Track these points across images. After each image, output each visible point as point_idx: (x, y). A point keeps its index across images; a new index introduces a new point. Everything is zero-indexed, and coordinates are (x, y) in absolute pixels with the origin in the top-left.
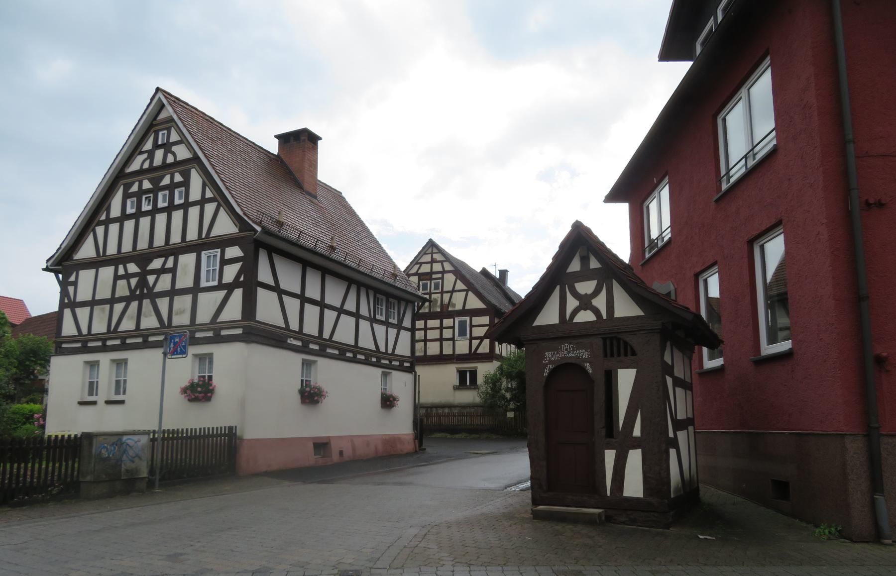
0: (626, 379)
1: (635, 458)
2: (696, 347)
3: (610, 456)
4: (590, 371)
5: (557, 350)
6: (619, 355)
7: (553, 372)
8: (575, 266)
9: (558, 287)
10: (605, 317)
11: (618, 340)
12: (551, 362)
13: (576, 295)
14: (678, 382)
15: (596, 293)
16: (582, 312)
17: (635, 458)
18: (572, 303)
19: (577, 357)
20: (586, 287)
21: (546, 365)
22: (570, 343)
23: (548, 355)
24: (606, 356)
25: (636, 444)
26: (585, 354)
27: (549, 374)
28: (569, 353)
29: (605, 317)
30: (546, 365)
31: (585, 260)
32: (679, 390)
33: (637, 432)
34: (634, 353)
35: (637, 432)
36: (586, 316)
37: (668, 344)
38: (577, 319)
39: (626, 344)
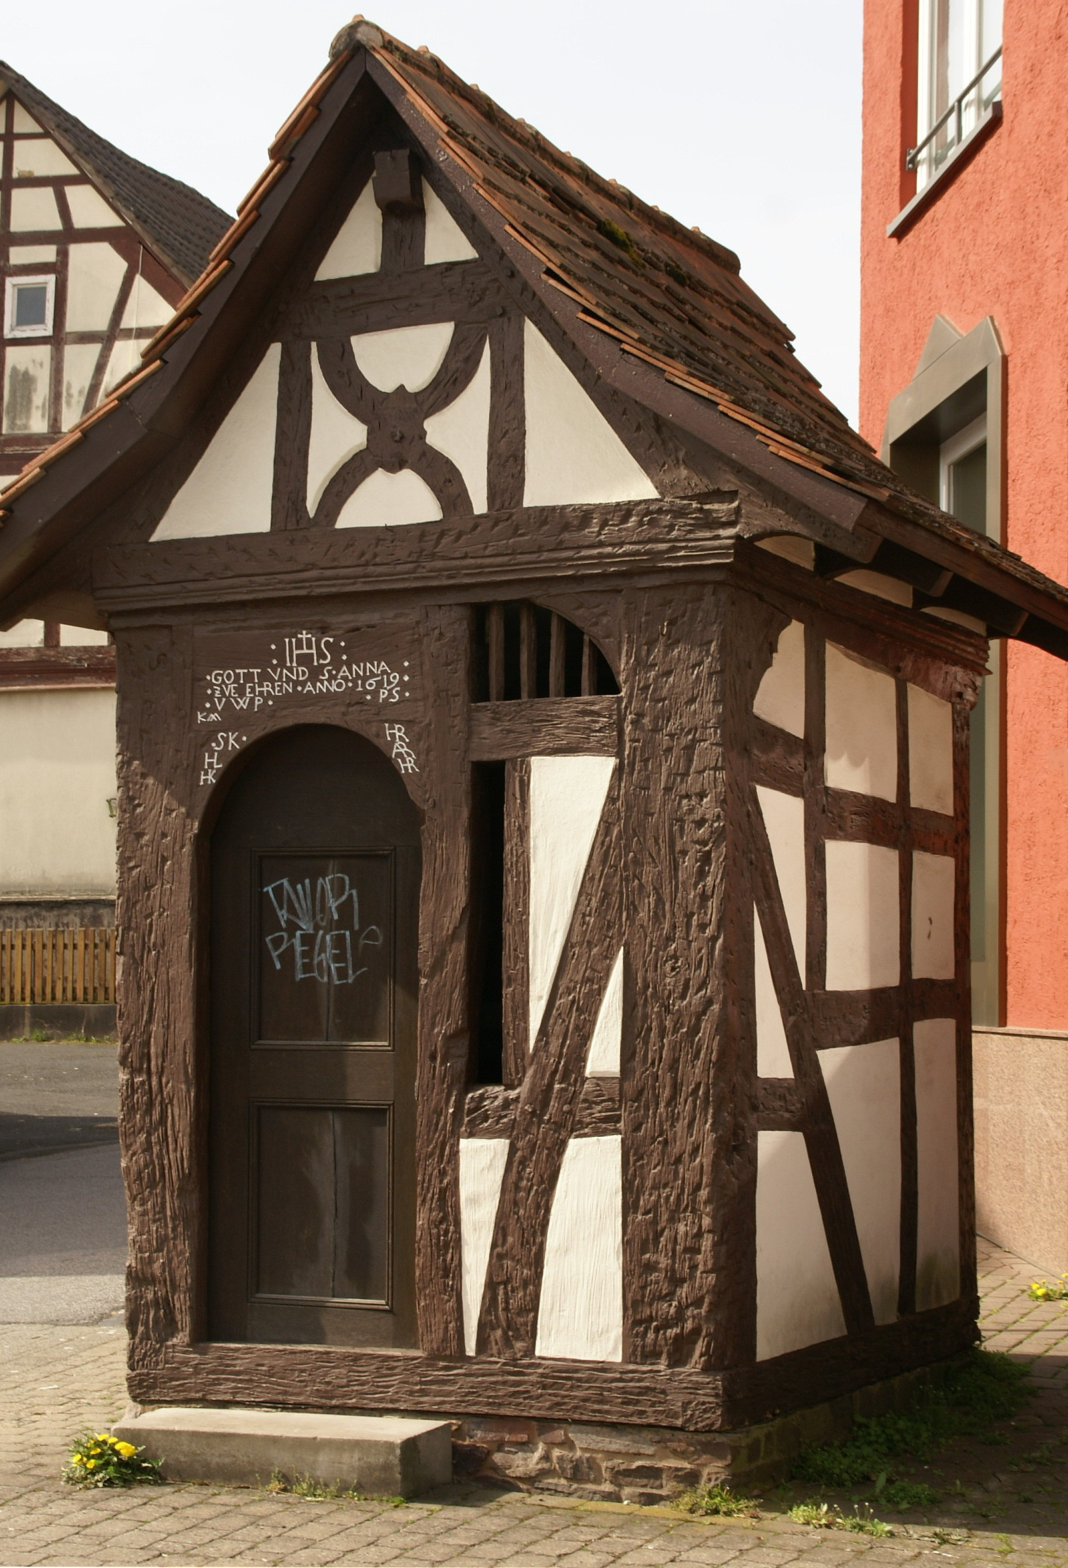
0: (566, 801)
1: (591, 1172)
2: (994, 644)
4: (408, 765)
5: (262, 658)
6: (541, 690)
7: (240, 769)
8: (356, 249)
9: (275, 351)
10: (480, 505)
11: (542, 617)
12: (233, 719)
13: (354, 393)
14: (829, 816)
15: (448, 384)
16: (379, 477)
17: (591, 1172)
20: (400, 357)
21: (211, 732)
22: (324, 630)
23: (222, 683)
24: (480, 692)
27: (224, 778)
28: (315, 674)
29: (480, 505)
30: (211, 732)
31: (403, 219)
32: (849, 860)
33: (604, 1055)
34: (606, 683)
35: (604, 1055)
36: (394, 501)
37: (792, 637)
38: (351, 516)
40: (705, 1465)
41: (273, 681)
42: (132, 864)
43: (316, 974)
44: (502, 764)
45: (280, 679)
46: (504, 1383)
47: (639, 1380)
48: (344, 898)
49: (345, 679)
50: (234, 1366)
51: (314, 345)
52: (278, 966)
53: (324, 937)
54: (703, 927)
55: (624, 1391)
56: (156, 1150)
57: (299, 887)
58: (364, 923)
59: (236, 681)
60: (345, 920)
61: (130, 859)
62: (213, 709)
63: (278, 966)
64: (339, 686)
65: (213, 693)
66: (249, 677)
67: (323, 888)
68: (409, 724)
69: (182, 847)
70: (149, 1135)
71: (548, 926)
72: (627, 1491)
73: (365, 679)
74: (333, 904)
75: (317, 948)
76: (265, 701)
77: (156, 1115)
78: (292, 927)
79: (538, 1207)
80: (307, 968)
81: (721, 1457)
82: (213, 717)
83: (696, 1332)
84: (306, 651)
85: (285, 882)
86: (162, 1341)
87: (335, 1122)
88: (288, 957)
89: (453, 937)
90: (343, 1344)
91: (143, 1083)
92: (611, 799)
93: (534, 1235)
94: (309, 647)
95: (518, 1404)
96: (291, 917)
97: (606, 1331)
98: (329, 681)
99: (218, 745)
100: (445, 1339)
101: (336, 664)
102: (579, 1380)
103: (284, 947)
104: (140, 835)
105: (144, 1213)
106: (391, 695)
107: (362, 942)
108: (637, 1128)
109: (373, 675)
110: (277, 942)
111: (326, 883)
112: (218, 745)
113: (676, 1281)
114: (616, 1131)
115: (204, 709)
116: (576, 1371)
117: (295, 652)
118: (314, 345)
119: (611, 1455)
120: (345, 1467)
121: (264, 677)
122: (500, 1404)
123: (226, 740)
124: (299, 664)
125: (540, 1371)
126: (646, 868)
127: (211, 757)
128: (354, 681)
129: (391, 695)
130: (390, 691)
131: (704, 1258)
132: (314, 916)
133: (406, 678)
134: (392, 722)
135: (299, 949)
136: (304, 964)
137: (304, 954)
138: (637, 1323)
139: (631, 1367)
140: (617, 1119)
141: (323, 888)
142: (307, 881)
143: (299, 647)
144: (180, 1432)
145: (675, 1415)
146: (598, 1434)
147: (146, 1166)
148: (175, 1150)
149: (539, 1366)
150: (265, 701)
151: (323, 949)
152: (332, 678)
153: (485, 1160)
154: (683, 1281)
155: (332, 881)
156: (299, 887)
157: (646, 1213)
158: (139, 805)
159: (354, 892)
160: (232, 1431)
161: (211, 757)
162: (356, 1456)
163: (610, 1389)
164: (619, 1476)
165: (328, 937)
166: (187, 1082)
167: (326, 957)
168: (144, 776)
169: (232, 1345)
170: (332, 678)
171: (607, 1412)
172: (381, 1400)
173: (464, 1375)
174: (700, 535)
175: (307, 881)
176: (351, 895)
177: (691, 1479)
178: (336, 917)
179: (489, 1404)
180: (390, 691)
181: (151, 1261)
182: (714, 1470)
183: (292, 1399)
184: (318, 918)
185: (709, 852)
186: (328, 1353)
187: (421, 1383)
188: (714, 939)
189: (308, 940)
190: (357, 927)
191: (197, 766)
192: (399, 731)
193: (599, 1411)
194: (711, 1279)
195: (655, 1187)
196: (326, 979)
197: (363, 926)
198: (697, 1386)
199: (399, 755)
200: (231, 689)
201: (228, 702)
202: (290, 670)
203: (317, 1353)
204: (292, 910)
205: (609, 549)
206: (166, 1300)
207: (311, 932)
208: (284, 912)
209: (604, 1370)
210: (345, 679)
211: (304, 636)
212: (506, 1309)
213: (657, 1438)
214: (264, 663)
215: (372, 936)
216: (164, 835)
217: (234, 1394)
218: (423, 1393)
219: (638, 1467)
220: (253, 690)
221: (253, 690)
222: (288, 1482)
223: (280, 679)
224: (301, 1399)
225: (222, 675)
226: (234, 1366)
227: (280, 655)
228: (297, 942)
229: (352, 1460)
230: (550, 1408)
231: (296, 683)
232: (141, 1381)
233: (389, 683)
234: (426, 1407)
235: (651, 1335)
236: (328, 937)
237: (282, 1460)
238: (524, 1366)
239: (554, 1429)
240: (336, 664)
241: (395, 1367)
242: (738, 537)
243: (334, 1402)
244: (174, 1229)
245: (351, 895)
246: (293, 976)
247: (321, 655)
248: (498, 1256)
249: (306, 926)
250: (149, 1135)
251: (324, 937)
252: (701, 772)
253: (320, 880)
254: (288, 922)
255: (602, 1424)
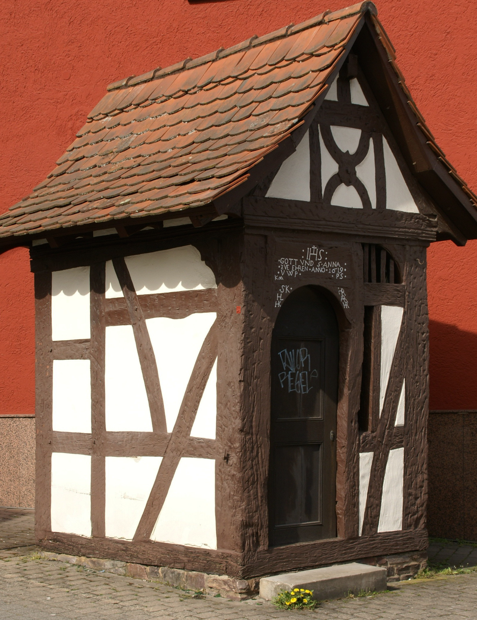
3: (366, 460)
4: (346, 305)
5: (298, 255)
10: (374, 206)
12: (288, 280)
18: (329, 167)
19: (327, 276)
23: (284, 263)
25: (397, 438)
26: (338, 270)
27: (284, 304)
29: (374, 206)
33: (400, 420)
35: (400, 420)
36: (346, 198)
39: (389, 257)
40: (421, 562)
41: (301, 265)
42: (248, 341)
43: (296, 390)
44: (373, 307)
45: (304, 265)
46: (369, 545)
47: (407, 536)
48: (306, 358)
49: (325, 267)
50: (282, 556)
51: (319, 125)
52: (282, 387)
53: (299, 374)
54: (424, 371)
55: (403, 540)
56: (255, 468)
57: (290, 353)
58: (312, 369)
59: (289, 264)
60: (306, 368)
61: (248, 338)
62: (280, 275)
63: (282, 387)
64: (323, 270)
65: (281, 268)
66: (293, 262)
67: (299, 354)
68: (346, 289)
69: (268, 334)
70: (252, 461)
71: (385, 370)
72: (402, 576)
73: (332, 268)
74: (302, 360)
75: (296, 379)
76: (299, 274)
77: (255, 453)
78: (288, 370)
79: (381, 476)
80: (293, 387)
81: (425, 558)
82: (281, 278)
83: (422, 516)
84: (314, 254)
85: (286, 350)
86: (255, 551)
87: (302, 450)
88: (286, 382)
89: (358, 375)
90: (306, 541)
91: (250, 439)
92: (403, 323)
93: (379, 487)
94: (315, 253)
95: (373, 552)
96: (288, 366)
97: (398, 520)
98: (320, 267)
99: (282, 291)
100: (354, 532)
101: (323, 261)
102: (391, 539)
103: (285, 378)
104: (252, 328)
105: (249, 496)
106: (340, 276)
107: (311, 376)
108: (407, 445)
109: (335, 267)
110: (282, 376)
111: (300, 351)
112: (282, 291)
113: (416, 498)
114: (402, 446)
115: (277, 274)
116: (390, 536)
117: (310, 254)
118: (319, 125)
119: (397, 564)
120: (370, 583)
121: (299, 263)
122: (368, 553)
123: (285, 288)
124: (311, 260)
125: (380, 538)
126: (410, 349)
127: (279, 295)
128: (328, 269)
129: (340, 276)
130: (340, 274)
131: (425, 489)
132: (295, 365)
133: (345, 270)
134: (341, 287)
135: (290, 379)
136: (292, 385)
137: (292, 381)
138: (406, 515)
139: (405, 531)
140: (402, 442)
141: (299, 354)
142: (293, 350)
143: (312, 252)
144: (317, 582)
145: (416, 546)
146: (394, 558)
147: (252, 475)
148: (263, 467)
149: (379, 536)
150: (299, 274)
151: (298, 379)
152: (321, 266)
153: (367, 460)
154: (418, 498)
155: (302, 350)
156: (290, 353)
157: (409, 475)
158: (251, 314)
159: (309, 355)
160: (331, 577)
161: (279, 295)
162: (374, 578)
163: (399, 541)
164: (400, 571)
165: (300, 374)
166: (268, 438)
167: (300, 382)
168: (253, 301)
169: (282, 547)
170: (321, 266)
171: (399, 549)
172: (332, 560)
173: (358, 544)
174: (428, 229)
175: (293, 350)
176: (308, 357)
177: (417, 567)
178: (303, 366)
179: (365, 553)
180: (340, 274)
181: (252, 517)
182: (423, 562)
183: (303, 565)
184: (297, 366)
185: (425, 344)
186: (315, 544)
187: (345, 550)
188: (427, 375)
189: (293, 375)
190: (310, 370)
191: (274, 300)
192: (342, 291)
193: (396, 549)
194: (427, 496)
195: (412, 466)
196: (299, 392)
197: (312, 370)
198: (423, 534)
199: (343, 300)
200: (287, 267)
201: (286, 273)
202: (308, 261)
203: (312, 545)
204: (288, 363)
205: (407, 230)
206: (257, 533)
207: (294, 372)
208: (285, 363)
209: (397, 534)
210: (325, 267)
211: (314, 247)
212: (371, 517)
213: (410, 555)
214: (299, 258)
215: (314, 374)
216: (261, 329)
217: (282, 568)
218: (345, 554)
219: (406, 567)
220: (294, 267)
221: (294, 267)
222: (355, 593)
223: (304, 265)
224: (306, 565)
225: (284, 260)
226: (282, 556)
227: (305, 254)
228: (289, 376)
229: (372, 579)
230: (383, 551)
231: (309, 267)
232: (248, 569)
233: (340, 271)
234: (346, 559)
235: (409, 519)
236: (300, 374)
237: (351, 585)
238: (375, 537)
239: (382, 559)
240: (323, 261)
241: (336, 546)
242: (437, 232)
243: (317, 563)
244: (262, 501)
245: (308, 357)
246: (288, 391)
247: (319, 257)
248: (369, 496)
249: (293, 369)
250: (252, 461)
251: (299, 374)
252: (423, 315)
253: (298, 350)
254: (286, 367)
255: (391, 554)
